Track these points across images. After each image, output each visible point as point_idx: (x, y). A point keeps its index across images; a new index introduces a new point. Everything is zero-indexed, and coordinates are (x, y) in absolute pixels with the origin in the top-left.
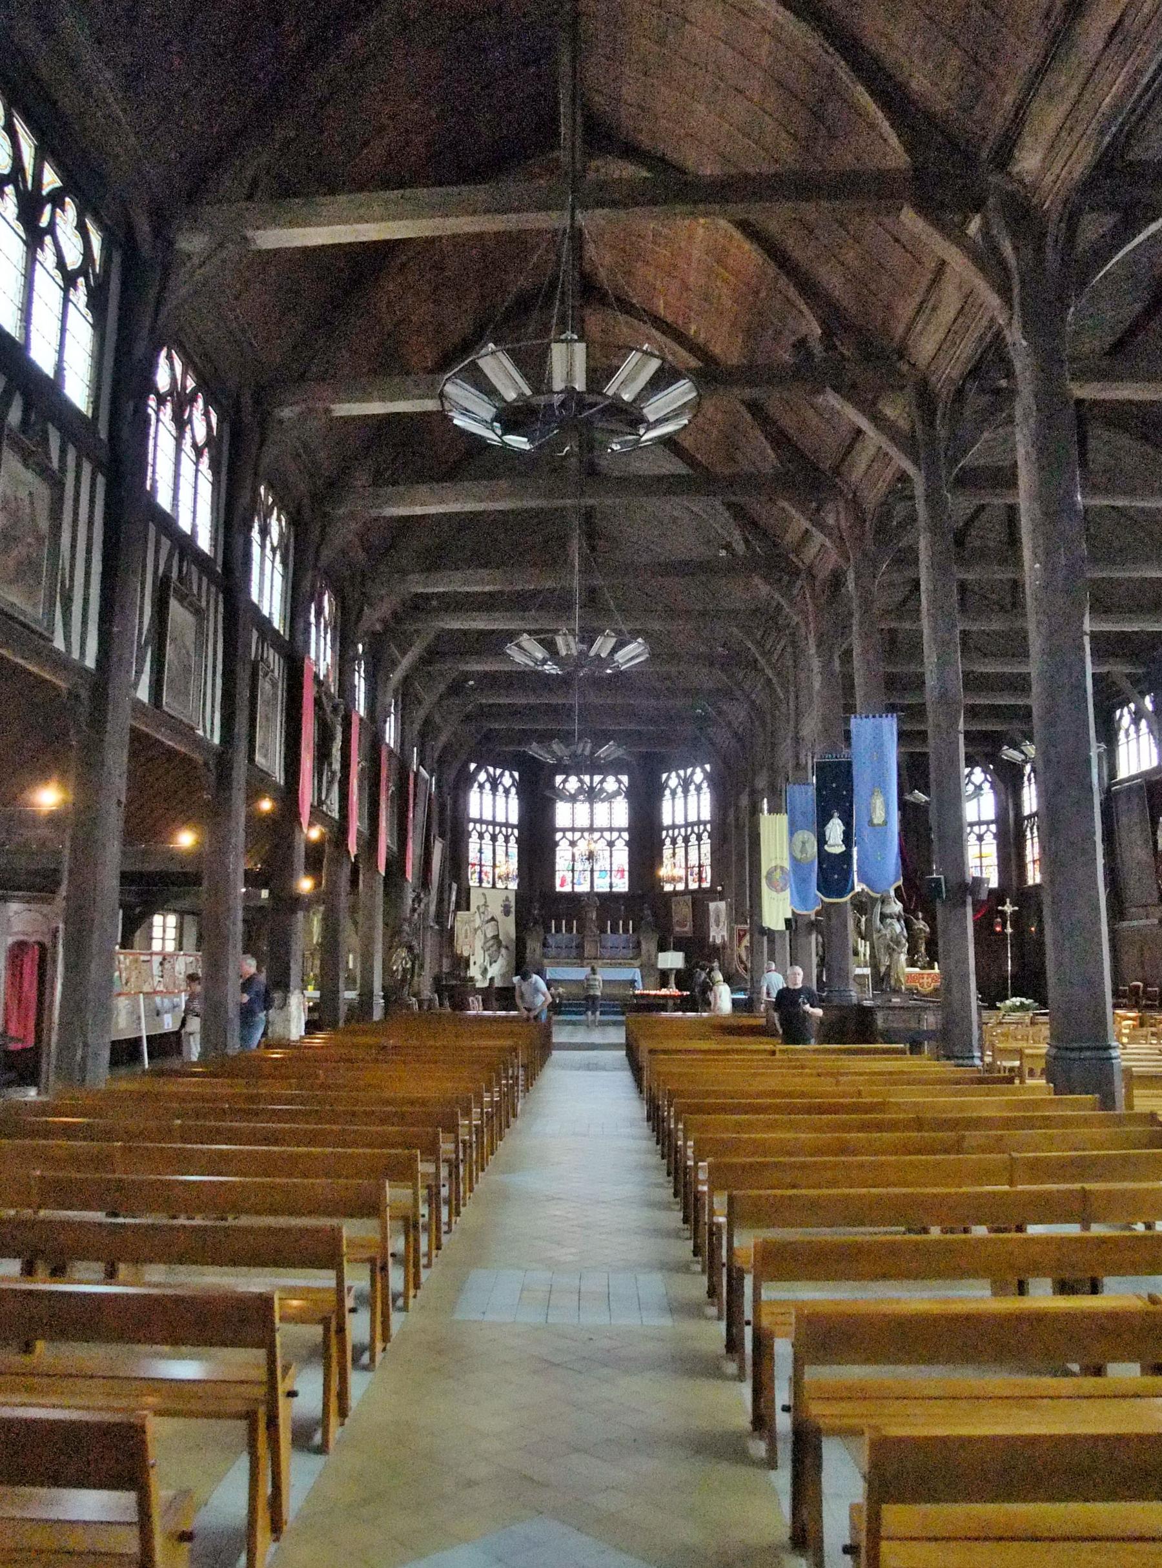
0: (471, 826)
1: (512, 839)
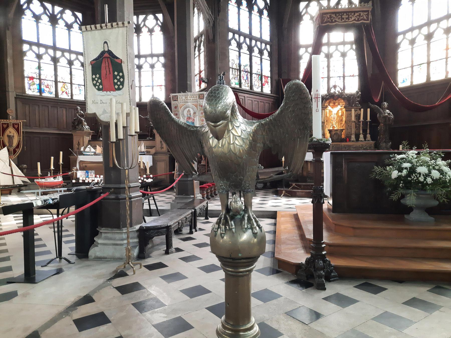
0: (231, 35)
1: (266, 53)
